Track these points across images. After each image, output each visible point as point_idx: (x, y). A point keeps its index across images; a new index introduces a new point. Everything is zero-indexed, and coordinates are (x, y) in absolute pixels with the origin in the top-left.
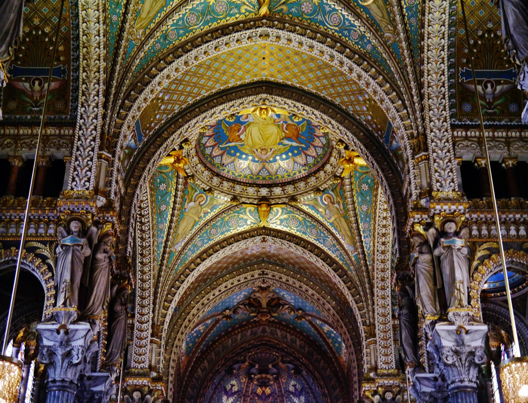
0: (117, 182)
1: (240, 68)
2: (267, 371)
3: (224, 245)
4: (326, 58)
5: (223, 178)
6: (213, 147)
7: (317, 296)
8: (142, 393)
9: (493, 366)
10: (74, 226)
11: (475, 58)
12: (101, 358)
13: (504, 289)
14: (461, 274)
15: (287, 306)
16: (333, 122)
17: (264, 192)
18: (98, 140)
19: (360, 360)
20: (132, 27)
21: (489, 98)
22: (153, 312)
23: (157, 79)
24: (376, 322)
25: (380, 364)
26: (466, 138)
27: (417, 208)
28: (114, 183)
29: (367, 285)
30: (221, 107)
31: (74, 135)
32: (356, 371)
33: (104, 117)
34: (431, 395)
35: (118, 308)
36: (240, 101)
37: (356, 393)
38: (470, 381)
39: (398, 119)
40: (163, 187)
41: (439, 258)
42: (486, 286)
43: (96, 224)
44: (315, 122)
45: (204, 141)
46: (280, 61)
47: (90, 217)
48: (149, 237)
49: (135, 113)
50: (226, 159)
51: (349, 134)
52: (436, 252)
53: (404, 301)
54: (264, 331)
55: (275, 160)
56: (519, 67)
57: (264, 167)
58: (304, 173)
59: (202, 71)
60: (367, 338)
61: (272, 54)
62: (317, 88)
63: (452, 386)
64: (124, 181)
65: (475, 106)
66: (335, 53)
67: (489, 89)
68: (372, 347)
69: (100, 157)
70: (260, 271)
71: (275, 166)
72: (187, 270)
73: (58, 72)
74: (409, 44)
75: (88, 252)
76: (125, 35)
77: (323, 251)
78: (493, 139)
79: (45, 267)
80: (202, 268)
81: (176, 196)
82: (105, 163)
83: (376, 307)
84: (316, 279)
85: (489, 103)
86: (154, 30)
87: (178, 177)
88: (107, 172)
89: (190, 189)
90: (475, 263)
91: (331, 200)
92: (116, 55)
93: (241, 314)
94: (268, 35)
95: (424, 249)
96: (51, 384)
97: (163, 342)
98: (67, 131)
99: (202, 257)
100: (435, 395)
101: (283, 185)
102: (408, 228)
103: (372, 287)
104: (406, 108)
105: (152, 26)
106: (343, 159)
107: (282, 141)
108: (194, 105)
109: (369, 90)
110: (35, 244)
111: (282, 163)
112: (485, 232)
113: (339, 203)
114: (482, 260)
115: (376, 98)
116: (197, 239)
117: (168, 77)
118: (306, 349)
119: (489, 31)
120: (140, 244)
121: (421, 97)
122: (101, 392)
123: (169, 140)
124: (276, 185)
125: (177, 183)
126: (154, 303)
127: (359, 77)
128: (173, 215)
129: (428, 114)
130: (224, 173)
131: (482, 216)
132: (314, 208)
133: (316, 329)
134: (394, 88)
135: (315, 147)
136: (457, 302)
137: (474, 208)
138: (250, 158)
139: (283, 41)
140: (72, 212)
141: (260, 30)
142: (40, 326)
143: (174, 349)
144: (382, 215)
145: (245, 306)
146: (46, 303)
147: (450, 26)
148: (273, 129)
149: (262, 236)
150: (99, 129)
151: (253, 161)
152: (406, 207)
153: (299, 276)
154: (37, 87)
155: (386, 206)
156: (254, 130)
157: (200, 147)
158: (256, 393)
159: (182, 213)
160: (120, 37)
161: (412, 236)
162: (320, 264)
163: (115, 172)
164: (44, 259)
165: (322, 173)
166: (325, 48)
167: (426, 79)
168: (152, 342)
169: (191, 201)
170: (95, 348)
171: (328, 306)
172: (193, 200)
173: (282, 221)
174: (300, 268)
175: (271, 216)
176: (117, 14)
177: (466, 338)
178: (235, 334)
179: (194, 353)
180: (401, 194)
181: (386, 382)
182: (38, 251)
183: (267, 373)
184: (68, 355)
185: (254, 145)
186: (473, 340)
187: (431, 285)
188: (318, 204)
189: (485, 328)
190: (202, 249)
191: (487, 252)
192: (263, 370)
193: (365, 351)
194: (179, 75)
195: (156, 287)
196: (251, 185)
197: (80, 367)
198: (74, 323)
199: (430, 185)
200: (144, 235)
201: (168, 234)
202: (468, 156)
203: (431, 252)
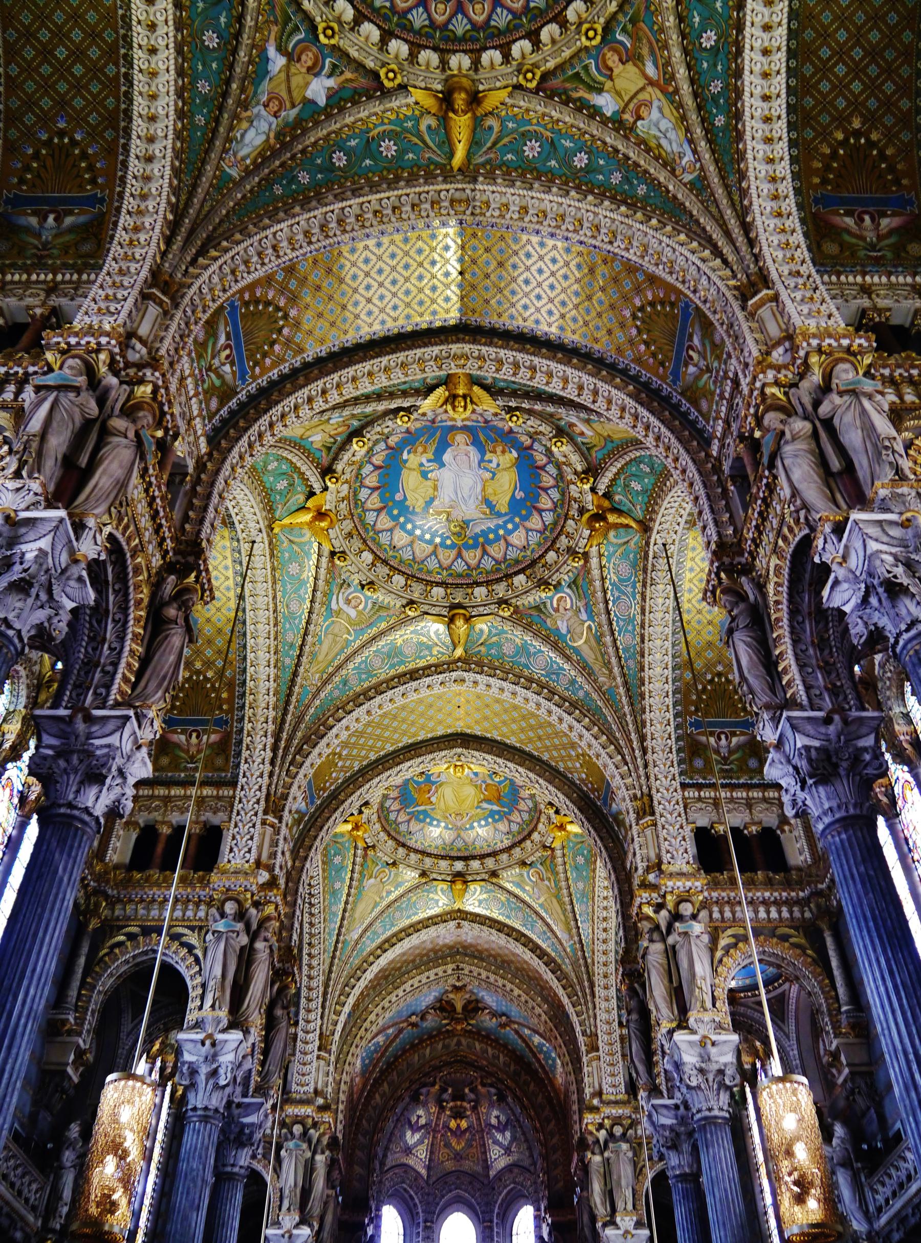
0: (283, 853)
1: (431, 719)
2: (462, 1098)
4: (531, 706)
5: (410, 849)
7: (524, 997)
8: (304, 1126)
9: (748, 1089)
10: (230, 908)
12: (255, 1078)
13: (755, 987)
14: (702, 968)
16: (541, 781)
17: (459, 866)
18: (263, 803)
19: (579, 1082)
20: (307, 671)
21: (724, 751)
22: (322, 1018)
23: (334, 731)
25: (605, 1087)
26: (700, 799)
27: (644, 885)
28: (279, 855)
30: (408, 764)
31: (234, 797)
32: (575, 1097)
33: (271, 775)
34: (671, 1128)
35: (279, 1012)
36: (431, 756)
37: (577, 1127)
38: (721, 1109)
39: (618, 777)
40: (337, 860)
41: (674, 947)
42: (733, 984)
43: (256, 904)
44: (519, 781)
45: (387, 804)
46: (478, 710)
47: (249, 896)
49: (307, 770)
50: (414, 826)
51: (560, 795)
52: (670, 940)
53: (633, 1004)
54: (459, 1043)
55: (472, 828)
56: (757, 714)
58: (507, 843)
59: (386, 721)
60: (588, 1052)
61: (468, 702)
62: (521, 741)
63: (698, 1116)
64: (292, 852)
65: (707, 761)
66: (542, 701)
67: (723, 742)
68: (594, 1064)
69: (264, 823)
70: (454, 966)
71: (472, 834)
73: (220, 723)
74: (628, 690)
75: (244, 940)
76: (299, 680)
77: (531, 940)
78: (732, 800)
79: (192, 959)
80: (383, 961)
81: (353, 871)
82: (269, 830)
83: (598, 1012)
85: (724, 758)
86: (332, 675)
87: (356, 848)
88: (272, 840)
89: (369, 863)
90: (719, 954)
92: (287, 703)
93: (431, 1021)
94: (463, 680)
95: (656, 936)
96: (190, 1113)
97: (333, 1058)
98: (226, 792)
99: (383, 948)
100: (677, 1128)
101: (482, 857)
102: (634, 910)
103: (592, 985)
104: (626, 764)
105: (331, 669)
108: (377, 761)
109: (583, 744)
110: (181, 930)
111: (480, 831)
112: (728, 914)
114: (727, 950)
115: (591, 753)
116: (378, 924)
117: (347, 728)
119: (719, 675)
121: (644, 751)
122: (253, 1124)
123: (347, 803)
124: (474, 857)
125: (355, 855)
126: (323, 1007)
127: (571, 728)
128: (348, 895)
129: (652, 771)
130: (411, 843)
131: (724, 894)
132: (518, 885)
133: (524, 1041)
134: (612, 740)
136: (699, 1004)
137: (714, 885)
139: (482, 687)
140: (228, 890)
141: (454, 674)
142: (182, 1036)
143: (346, 1067)
146: (191, 1005)
147: (674, 669)
148: (470, 791)
150: (264, 789)
151: (446, 828)
152: (630, 884)
154: (194, 740)
155: (606, 883)
156: (447, 791)
157: (383, 812)
159: (360, 893)
160: (293, 682)
161: (640, 920)
162: (527, 955)
163: (281, 842)
164: (190, 948)
165: (528, 842)
166: (529, 694)
167: (648, 730)
168: (318, 1057)
170: (247, 1065)
171: (538, 1010)
173: (480, 902)
174: (503, 961)
175: (467, 896)
176: (291, 657)
177: (713, 1051)
179: (371, 1073)
180: (624, 868)
182: (184, 939)
183: (463, 1099)
184: (214, 1073)
185: (447, 810)
186: (721, 1054)
187: (666, 982)
188: (524, 881)
189: (735, 1038)
190: (384, 937)
191: (733, 940)
192: (458, 1096)
193: (585, 1070)
194: (359, 726)
195: (326, 986)
196: (443, 857)
197: (228, 1090)
198: (223, 1031)
199: (659, 857)
201: (343, 919)
202: (703, 822)
203: (664, 940)
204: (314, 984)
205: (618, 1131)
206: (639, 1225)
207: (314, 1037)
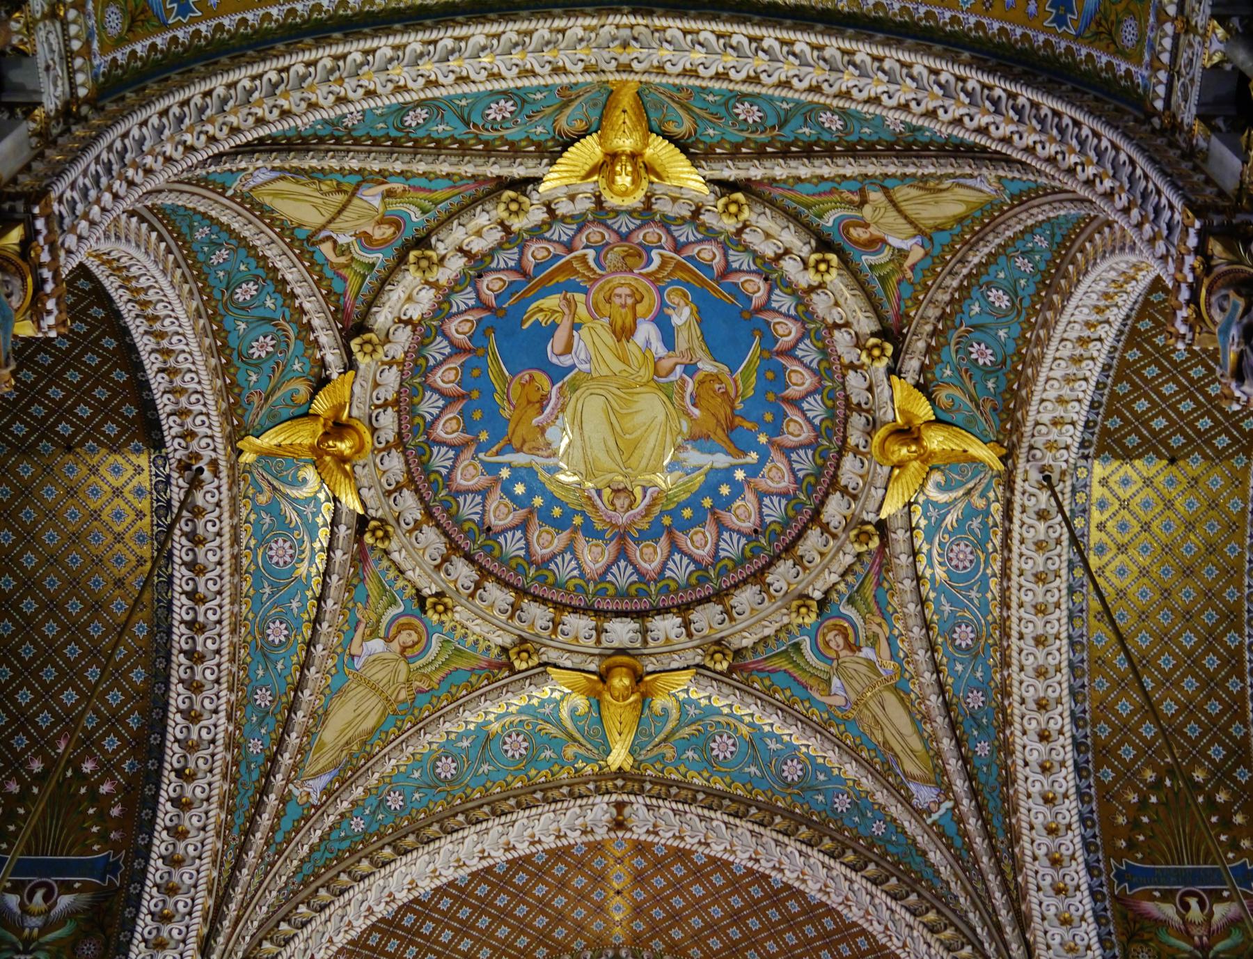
6: (458, 448)
11: (1148, 838)
17: (621, 632)
29: (999, 898)
48: (216, 711)
57: (622, 553)
91: (846, 637)
106: (882, 432)
107: (683, 455)
113: (873, 641)
120: (180, 736)
135: (787, 451)
138: (578, 520)
144: (1029, 631)
149: (614, 797)
169: (373, 634)
172: (382, 633)
200: (197, 699)
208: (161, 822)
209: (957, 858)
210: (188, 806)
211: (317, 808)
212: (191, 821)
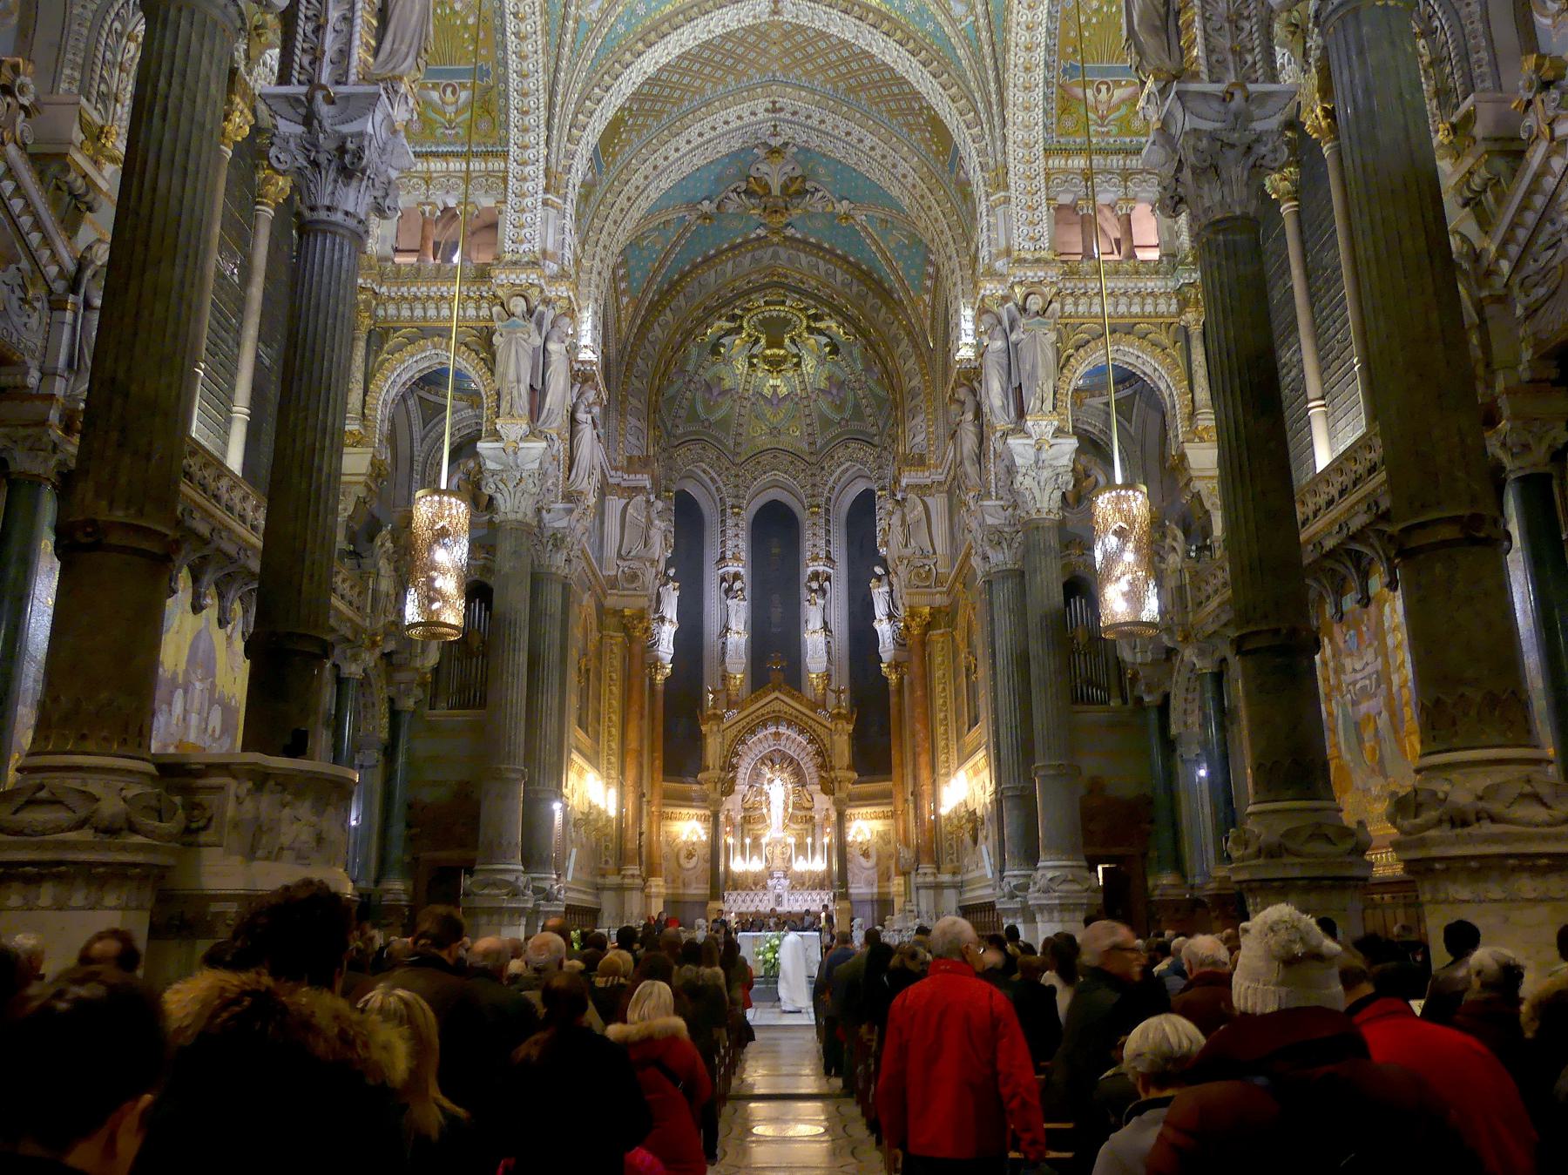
3: (693, 15)
15: (820, 194)
22: (547, 144)
24: (1011, 159)
29: (992, 86)
54: (775, 255)
60: (988, 195)
68: (1000, 210)
72: (617, 65)
84: (880, 112)
97: (570, 209)
100: (1225, 137)
118: (855, 289)
126: (549, 127)
145: (739, 194)
153: (845, 109)
158: (761, 394)
168: (545, 203)
178: (722, 262)
179: (645, 292)
181: (1030, 274)
204: (530, 84)
205: (1035, 303)
206: (1059, 432)
207: (536, 171)
208: (510, 49)
209: (973, 54)
210: (525, 38)
211: (597, 23)
212: (528, 48)
